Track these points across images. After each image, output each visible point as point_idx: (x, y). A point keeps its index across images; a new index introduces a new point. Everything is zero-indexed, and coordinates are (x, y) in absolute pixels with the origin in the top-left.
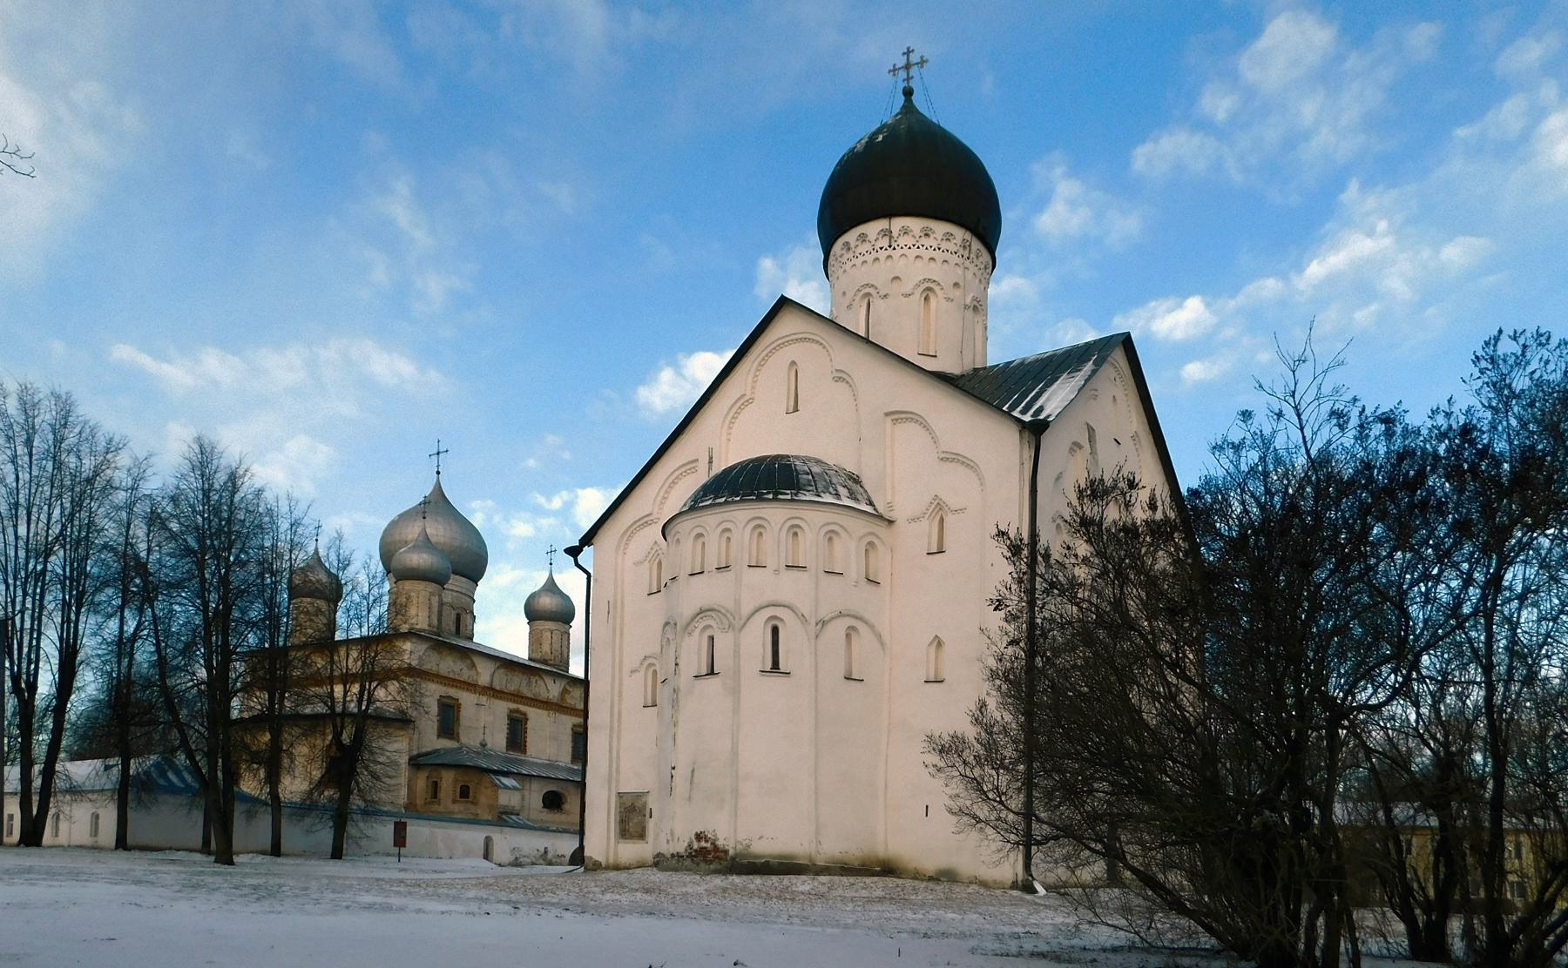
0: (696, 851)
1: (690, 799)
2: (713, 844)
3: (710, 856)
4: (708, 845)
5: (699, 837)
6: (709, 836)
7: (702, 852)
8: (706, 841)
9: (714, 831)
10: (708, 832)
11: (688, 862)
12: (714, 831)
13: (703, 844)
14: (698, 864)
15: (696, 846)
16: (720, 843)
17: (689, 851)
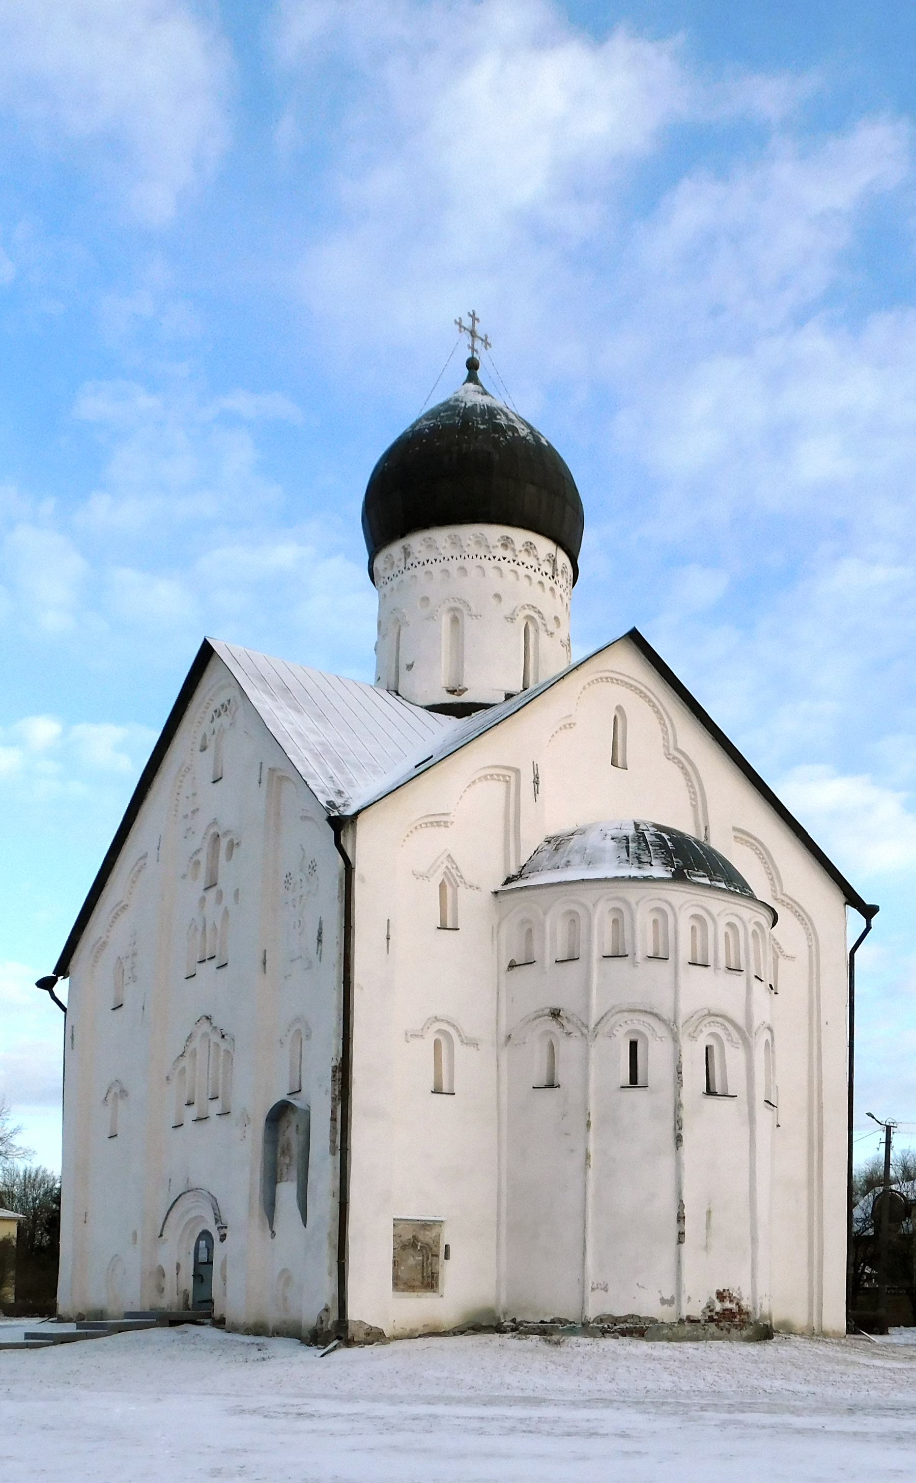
0: (717, 1313)
1: (707, 1248)
2: (737, 1304)
3: (737, 1320)
4: (733, 1306)
5: (721, 1296)
6: (735, 1295)
7: (727, 1315)
8: (731, 1301)
9: (739, 1289)
10: (733, 1289)
11: (712, 1327)
12: (739, 1289)
13: (728, 1305)
14: (729, 1331)
15: (718, 1307)
16: (744, 1303)
17: (709, 1314)
